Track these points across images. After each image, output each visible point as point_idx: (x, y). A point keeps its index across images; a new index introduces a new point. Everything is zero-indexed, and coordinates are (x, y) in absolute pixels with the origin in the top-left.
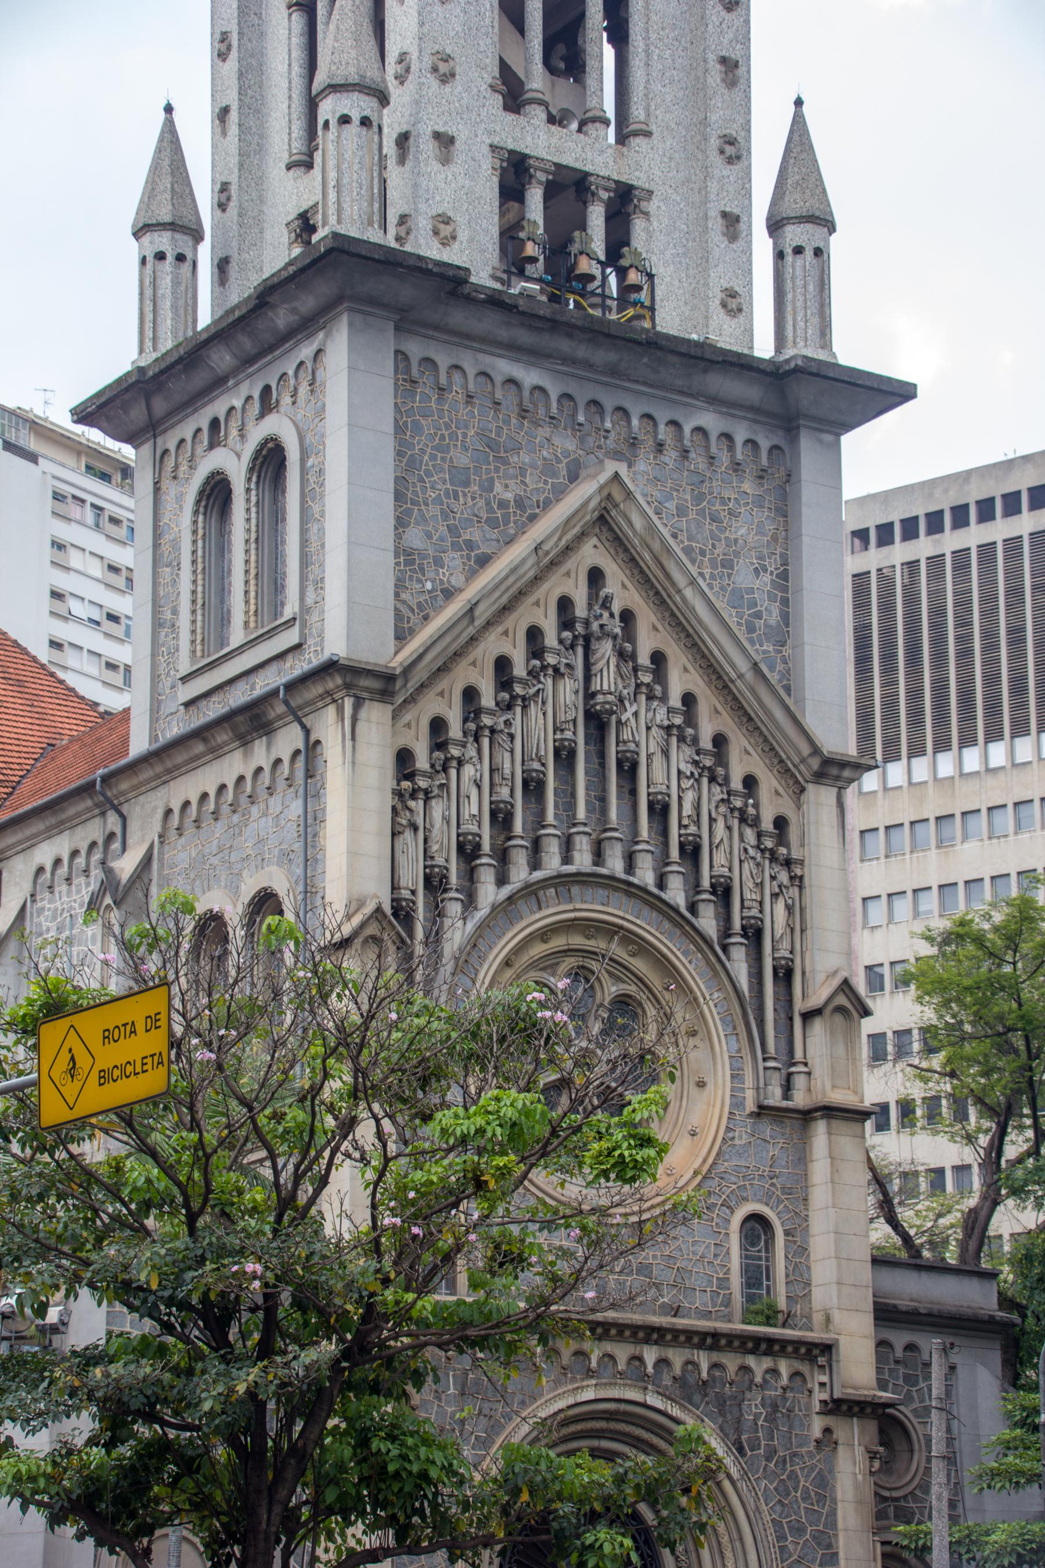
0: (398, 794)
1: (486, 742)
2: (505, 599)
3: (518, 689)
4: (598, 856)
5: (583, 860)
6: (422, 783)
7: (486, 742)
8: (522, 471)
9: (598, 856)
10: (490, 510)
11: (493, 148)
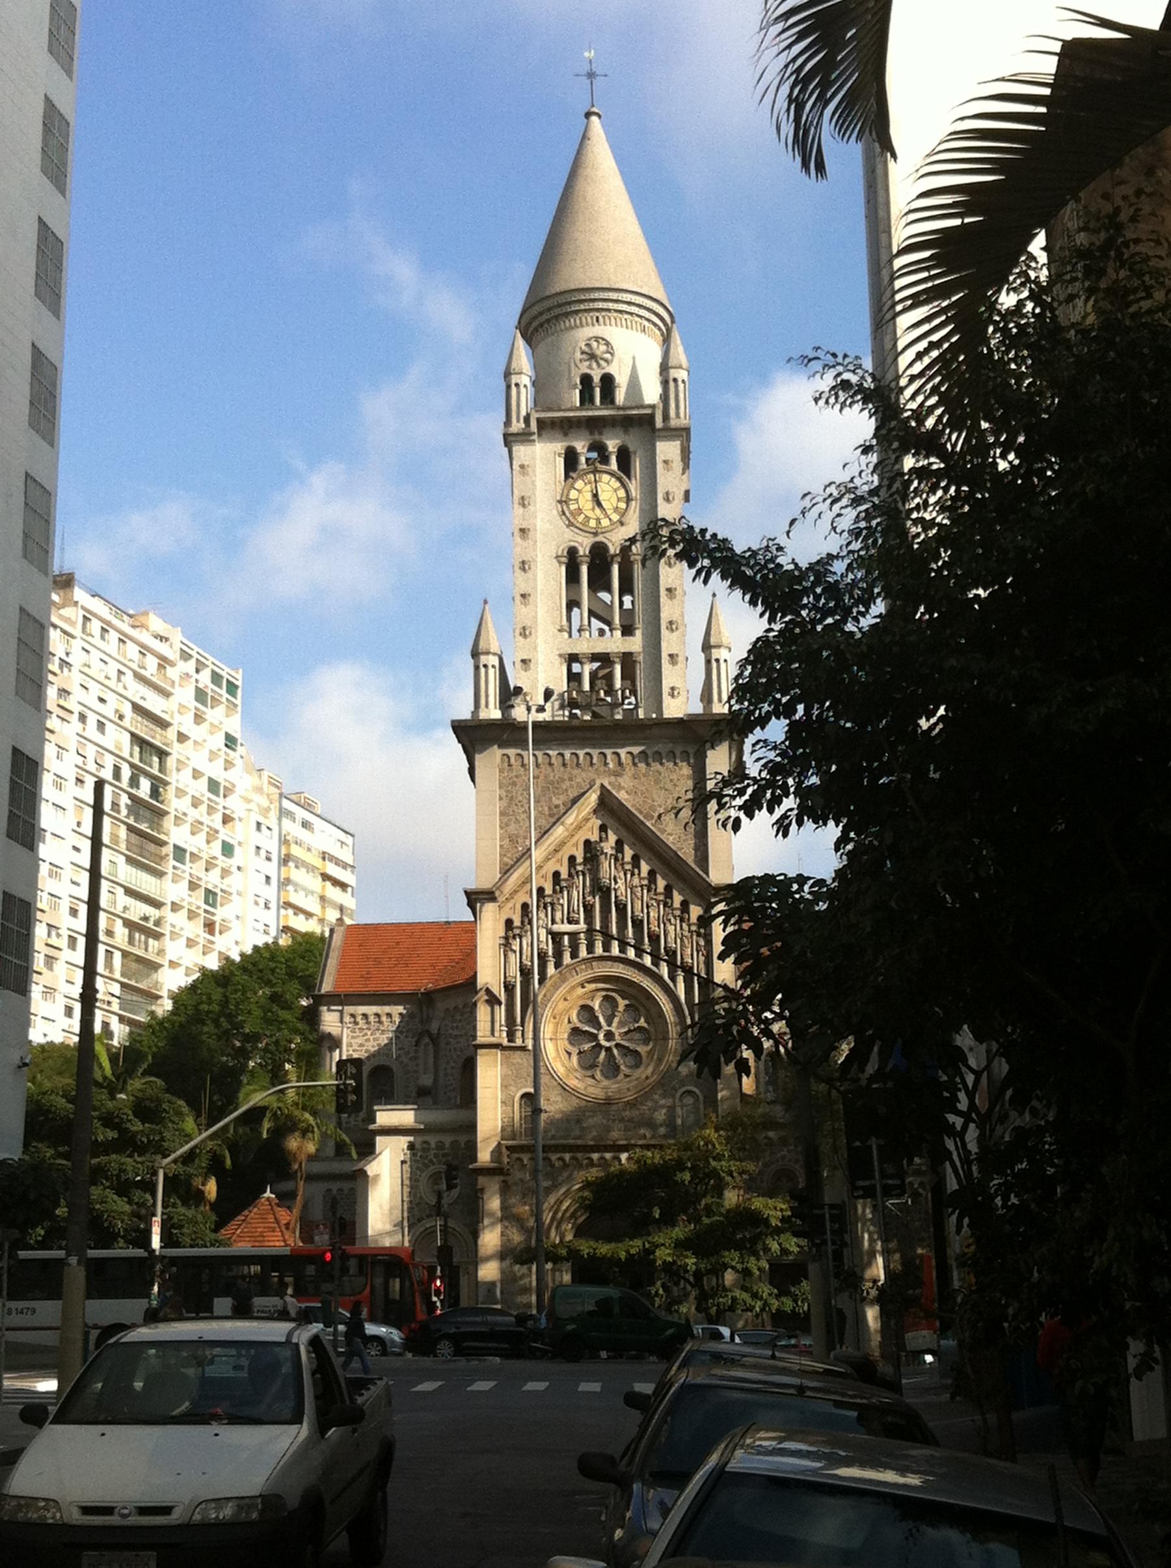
0: (506, 938)
1: (549, 909)
2: (552, 848)
3: (564, 884)
4: (607, 948)
5: (599, 950)
6: (517, 931)
7: (549, 909)
8: (566, 790)
9: (607, 948)
10: (550, 809)
11: (560, 656)
